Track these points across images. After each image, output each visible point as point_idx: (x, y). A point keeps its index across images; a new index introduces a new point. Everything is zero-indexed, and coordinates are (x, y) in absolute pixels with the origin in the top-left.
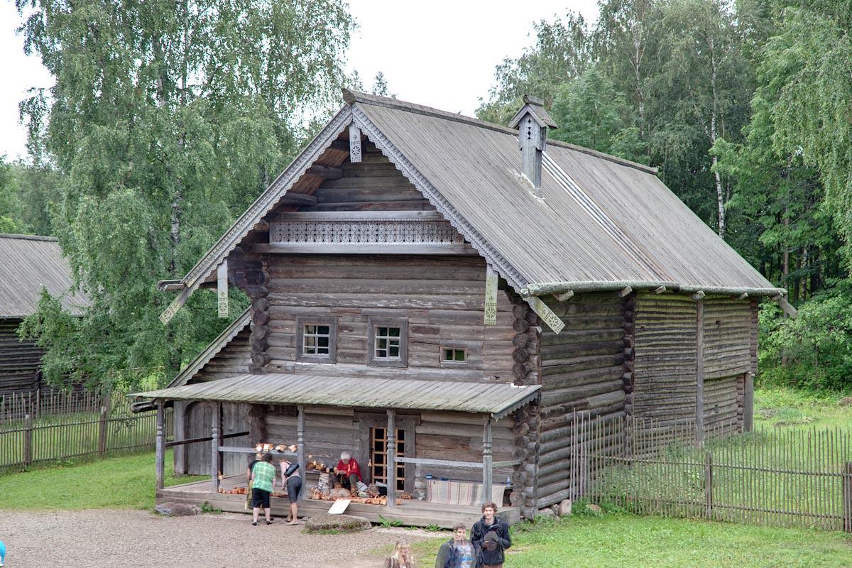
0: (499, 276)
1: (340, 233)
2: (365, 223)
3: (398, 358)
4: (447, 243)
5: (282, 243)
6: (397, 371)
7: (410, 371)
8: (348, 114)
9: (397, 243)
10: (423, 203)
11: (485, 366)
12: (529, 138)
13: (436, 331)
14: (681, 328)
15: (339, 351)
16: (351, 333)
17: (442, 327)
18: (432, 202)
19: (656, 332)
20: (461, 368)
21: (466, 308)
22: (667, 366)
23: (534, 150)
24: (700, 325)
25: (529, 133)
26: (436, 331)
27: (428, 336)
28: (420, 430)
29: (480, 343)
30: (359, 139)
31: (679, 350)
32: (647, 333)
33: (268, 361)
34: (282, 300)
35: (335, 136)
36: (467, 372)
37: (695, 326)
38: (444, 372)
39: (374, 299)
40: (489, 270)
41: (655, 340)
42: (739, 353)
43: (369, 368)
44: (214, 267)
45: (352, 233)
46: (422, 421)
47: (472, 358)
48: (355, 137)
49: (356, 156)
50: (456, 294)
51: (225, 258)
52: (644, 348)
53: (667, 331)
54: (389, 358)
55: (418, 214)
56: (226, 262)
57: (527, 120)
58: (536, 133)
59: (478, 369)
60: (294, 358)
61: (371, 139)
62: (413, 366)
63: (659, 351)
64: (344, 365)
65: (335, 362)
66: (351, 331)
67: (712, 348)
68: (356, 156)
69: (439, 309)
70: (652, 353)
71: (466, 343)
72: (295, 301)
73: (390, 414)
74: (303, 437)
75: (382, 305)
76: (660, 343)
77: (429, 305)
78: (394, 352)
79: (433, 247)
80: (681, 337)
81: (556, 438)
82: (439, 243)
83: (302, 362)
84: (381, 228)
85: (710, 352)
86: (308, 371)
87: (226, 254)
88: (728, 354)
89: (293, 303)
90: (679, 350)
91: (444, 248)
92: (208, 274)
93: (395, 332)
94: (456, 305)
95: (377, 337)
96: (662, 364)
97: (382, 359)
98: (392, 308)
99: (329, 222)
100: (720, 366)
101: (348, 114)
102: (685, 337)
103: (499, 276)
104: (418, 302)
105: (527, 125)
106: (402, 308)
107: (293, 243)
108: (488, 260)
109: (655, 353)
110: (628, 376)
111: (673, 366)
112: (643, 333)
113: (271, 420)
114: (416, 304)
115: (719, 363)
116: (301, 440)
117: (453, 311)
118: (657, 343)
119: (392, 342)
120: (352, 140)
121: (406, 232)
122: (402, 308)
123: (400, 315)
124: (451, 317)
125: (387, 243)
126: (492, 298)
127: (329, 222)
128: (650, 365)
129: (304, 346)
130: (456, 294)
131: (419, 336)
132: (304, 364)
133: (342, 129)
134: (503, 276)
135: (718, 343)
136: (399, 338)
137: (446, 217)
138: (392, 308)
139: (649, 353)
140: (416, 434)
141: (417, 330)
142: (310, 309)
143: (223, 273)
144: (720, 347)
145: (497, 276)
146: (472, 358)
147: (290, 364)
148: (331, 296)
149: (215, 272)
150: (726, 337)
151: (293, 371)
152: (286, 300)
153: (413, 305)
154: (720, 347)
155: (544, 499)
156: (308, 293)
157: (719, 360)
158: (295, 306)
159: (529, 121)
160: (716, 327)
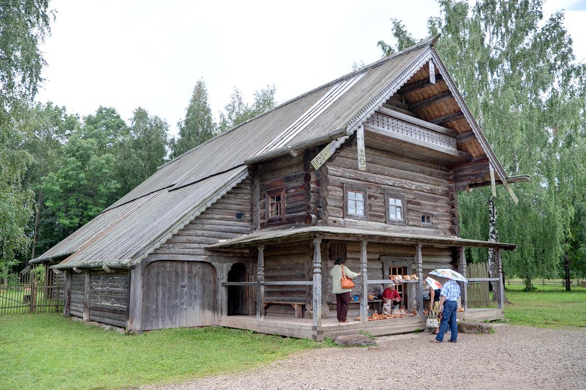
1: (401, 128)
11: (439, 226)
13: (419, 204)
16: (375, 200)
17: (421, 202)
20: (429, 227)
21: (429, 192)
26: (419, 204)
27: (415, 206)
30: (433, 70)
44: (356, 128)
59: (436, 228)
60: (341, 215)
66: (376, 199)
71: (432, 212)
75: (390, 184)
77: (414, 187)
94: (426, 189)
123: (400, 191)
124: (425, 196)
131: (410, 206)
132: (351, 220)
134: (496, 170)
138: (396, 187)
149: (355, 132)
152: (335, 171)
153: (406, 186)
156: (347, 168)
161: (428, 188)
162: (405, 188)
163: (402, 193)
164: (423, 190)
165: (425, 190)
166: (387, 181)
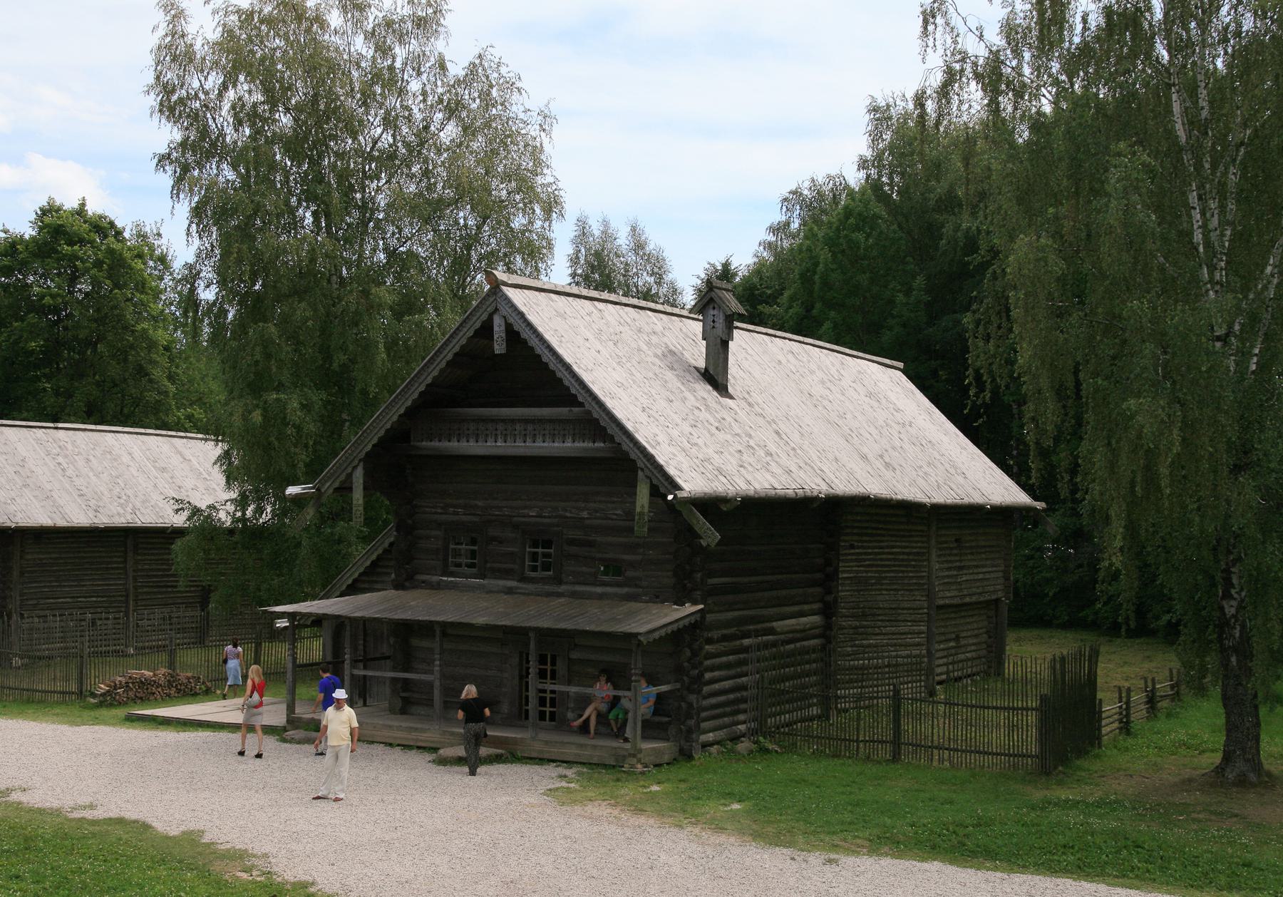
0: (651, 482)
2: (513, 421)
3: (551, 573)
4: (600, 445)
5: (424, 443)
6: (547, 588)
7: (563, 588)
8: (491, 300)
9: (546, 444)
10: (572, 401)
12: (714, 327)
14: (907, 547)
15: (488, 565)
18: (580, 399)
19: (870, 551)
22: (887, 590)
23: (719, 341)
24: (933, 542)
25: (714, 321)
26: (590, 544)
28: (575, 655)
29: (639, 558)
30: (503, 328)
31: (903, 572)
32: (857, 551)
33: (410, 577)
34: (427, 507)
35: (478, 325)
36: (625, 590)
37: (925, 545)
38: (599, 590)
39: (525, 507)
40: (640, 473)
41: (869, 560)
42: (987, 576)
43: (520, 585)
44: (349, 470)
45: (499, 432)
46: (576, 645)
47: (630, 573)
48: (500, 326)
49: (499, 347)
50: (614, 502)
51: (360, 460)
52: (854, 569)
53: (886, 550)
54: (539, 574)
55: (569, 411)
56: (361, 464)
57: (711, 306)
58: (721, 321)
59: (636, 586)
61: (516, 328)
62: (566, 583)
63: (876, 572)
64: (492, 582)
65: (483, 577)
66: (501, 542)
67: (949, 569)
68: (499, 347)
69: (595, 518)
70: (864, 575)
72: (442, 508)
73: (531, 635)
74: (440, 660)
75: (534, 514)
76: (875, 563)
77: (585, 514)
78: (546, 567)
79: (585, 449)
80: (906, 557)
81: (728, 666)
82: (591, 445)
83: (448, 576)
84: (530, 427)
85: (947, 573)
86: (453, 586)
87: (362, 455)
88: (972, 577)
89: (439, 511)
90: (903, 572)
91: (597, 449)
92: (343, 477)
93: (547, 544)
95: (528, 550)
96: (878, 587)
97: (533, 574)
98: (545, 517)
99: (474, 420)
100: (960, 590)
101: (491, 300)
102: (911, 557)
103: (651, 482)
104: (573, 511)
105: (712, 312)
106: (556, 517)
107: (435, 444)
108: (640, 464)
109: (869, 574)
110: (829, 598)
111: (895, 590)
112: (852, 551)
113: (415, 642)
114: (571, 512)
115: (958, 587)
116: (437, 663)
117: (610, 521)
118: (871, 562)
119: (545, 555)
120: (496, 328)
121: (556, 432)
122: (556, 517)
125: (536, 444)
126: (643, 506)
127: (474, 420)
128: (863, 588)
129: (450, 560)
130: (614, 502)
131: (574, 550)
132: (450, 579)
133: (485, 317)
134: (655, 482)
135: (958, 564)
136: (552, 551)
137: (595, 415)
138: (545, 517)
139: (860, 575)
140: (569, 659)
141: (572, 542)
142: (456, 518)
143: (359, 477)
144: (961, 568)
145: (648, 481)
146: (630, 573)
147: (435, 578)
148: (480, 504)
149: (350, 476)
150: (969, 557)
151: (438, 587)
153: (568, 514)
154: (961, 568)
155: (711, 734)
157: (960, 583)
158: (441, 514)
159: (714, 308)
160: (955, 545)
161: (619, 512)
162: (567, 517)
163: (555, 529)
164: (609, 516)
165: (615, 517)
166: (526, 511)
